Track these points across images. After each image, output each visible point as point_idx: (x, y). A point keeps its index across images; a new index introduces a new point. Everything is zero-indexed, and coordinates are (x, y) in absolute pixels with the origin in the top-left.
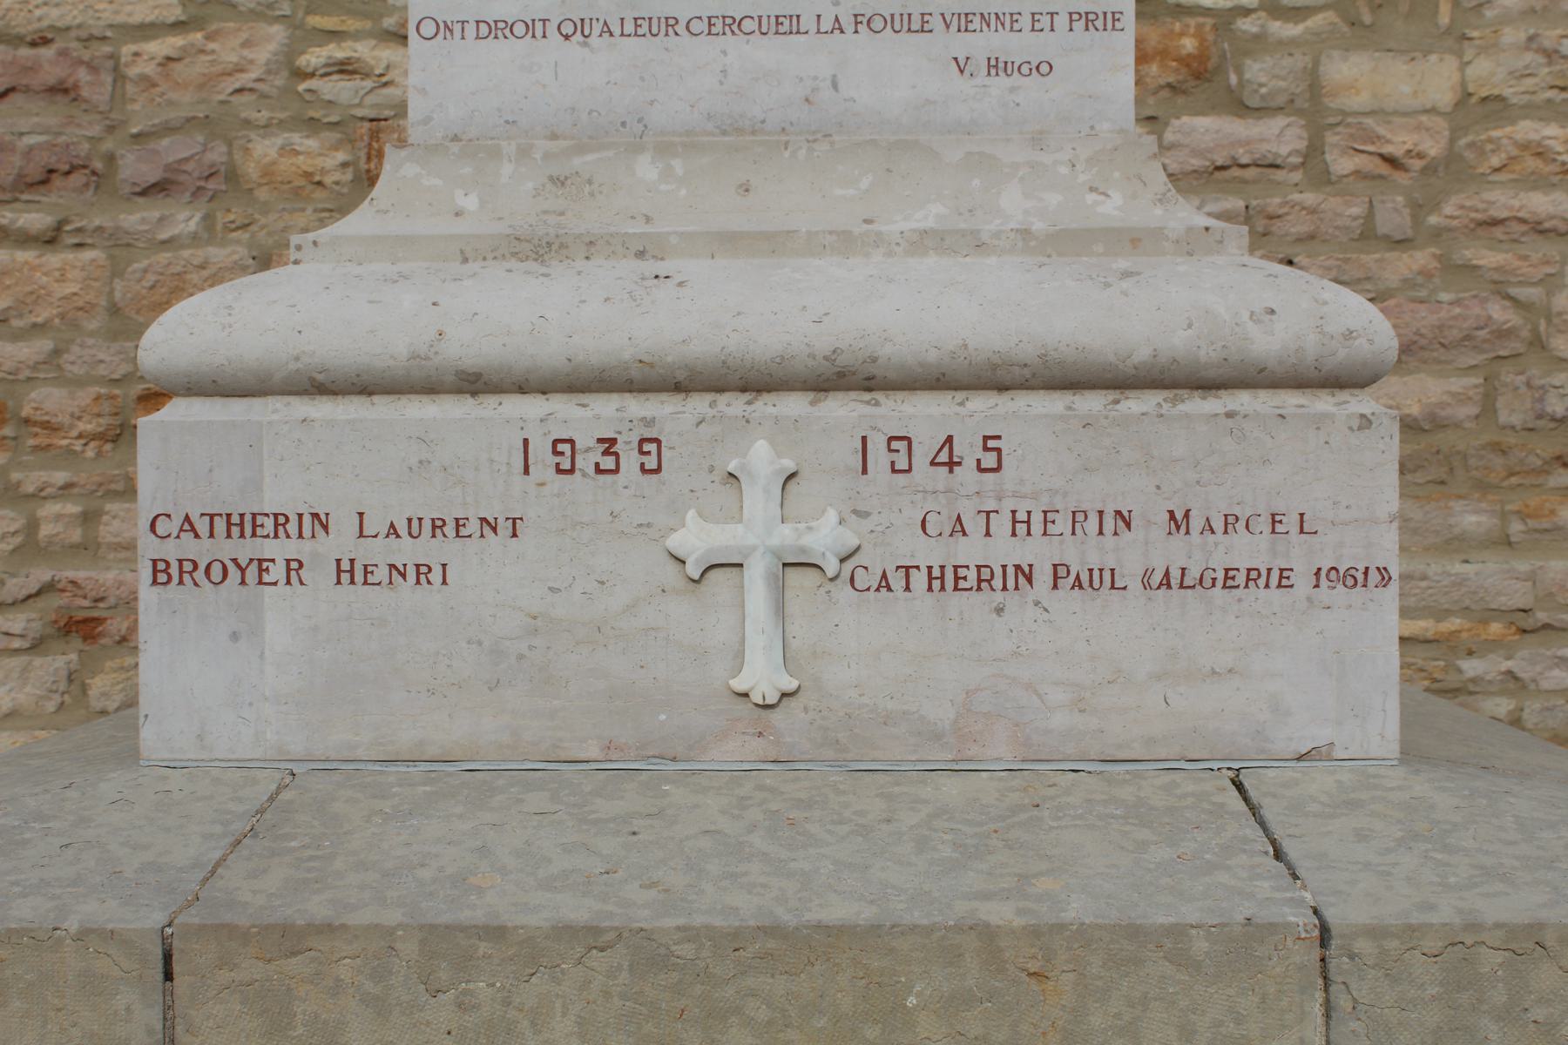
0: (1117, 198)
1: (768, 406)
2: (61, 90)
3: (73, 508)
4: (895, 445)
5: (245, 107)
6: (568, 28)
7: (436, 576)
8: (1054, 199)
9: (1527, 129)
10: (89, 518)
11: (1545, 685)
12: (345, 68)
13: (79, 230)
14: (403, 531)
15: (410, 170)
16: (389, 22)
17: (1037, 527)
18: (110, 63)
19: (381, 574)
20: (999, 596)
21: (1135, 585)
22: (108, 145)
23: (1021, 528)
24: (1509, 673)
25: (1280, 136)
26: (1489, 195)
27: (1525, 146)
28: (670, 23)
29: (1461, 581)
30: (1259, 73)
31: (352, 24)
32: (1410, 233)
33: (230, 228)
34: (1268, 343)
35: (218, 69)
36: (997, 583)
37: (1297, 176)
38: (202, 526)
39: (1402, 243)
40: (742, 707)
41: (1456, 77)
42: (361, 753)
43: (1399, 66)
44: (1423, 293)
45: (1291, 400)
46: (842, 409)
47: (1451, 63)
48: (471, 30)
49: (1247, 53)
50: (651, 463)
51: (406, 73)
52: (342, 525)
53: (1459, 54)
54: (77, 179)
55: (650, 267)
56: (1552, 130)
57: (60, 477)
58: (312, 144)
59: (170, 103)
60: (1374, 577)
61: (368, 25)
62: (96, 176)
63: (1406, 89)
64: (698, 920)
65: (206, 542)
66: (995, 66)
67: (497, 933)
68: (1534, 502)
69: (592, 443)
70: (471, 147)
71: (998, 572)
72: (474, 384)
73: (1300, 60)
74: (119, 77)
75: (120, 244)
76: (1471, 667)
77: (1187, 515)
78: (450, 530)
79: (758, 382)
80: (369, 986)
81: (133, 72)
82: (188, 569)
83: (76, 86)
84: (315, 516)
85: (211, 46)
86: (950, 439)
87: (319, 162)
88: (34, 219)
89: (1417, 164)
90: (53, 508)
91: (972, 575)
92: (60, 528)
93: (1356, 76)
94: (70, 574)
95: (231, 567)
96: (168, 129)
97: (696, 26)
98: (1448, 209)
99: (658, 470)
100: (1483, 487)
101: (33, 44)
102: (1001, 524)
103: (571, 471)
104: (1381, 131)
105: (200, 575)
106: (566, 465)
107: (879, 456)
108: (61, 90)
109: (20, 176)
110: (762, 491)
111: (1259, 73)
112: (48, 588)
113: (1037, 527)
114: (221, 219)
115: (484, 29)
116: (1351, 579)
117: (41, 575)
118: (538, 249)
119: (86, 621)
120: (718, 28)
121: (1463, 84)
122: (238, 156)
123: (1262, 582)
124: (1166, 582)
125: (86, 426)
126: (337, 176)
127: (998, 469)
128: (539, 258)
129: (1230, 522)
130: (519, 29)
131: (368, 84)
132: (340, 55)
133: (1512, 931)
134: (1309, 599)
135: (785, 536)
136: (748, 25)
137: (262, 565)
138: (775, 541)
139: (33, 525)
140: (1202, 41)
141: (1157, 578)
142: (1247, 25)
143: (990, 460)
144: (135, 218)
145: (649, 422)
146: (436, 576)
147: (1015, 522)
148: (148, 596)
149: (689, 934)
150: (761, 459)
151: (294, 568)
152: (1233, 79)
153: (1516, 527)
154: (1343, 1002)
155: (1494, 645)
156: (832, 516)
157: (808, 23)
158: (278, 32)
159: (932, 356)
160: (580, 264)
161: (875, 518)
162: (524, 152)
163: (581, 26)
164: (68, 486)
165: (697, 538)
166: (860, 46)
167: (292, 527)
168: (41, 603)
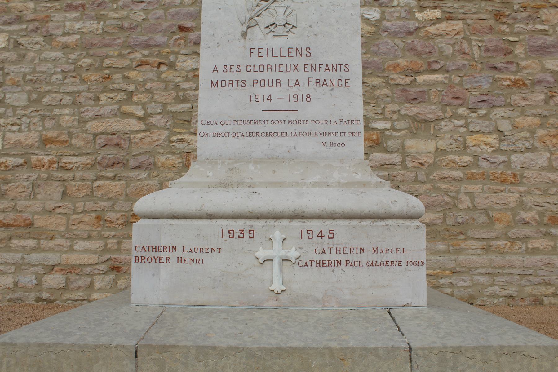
0: (360, 175)
1: (280, 223)
2: (117, 145)
3: (115, 241)
4: (309, 232)
5: (159, 149)
6: (234, 135)
7: (201, 262)
8: (345, 175)
9: (451, 157)
10: (119, 243)
11: (459, 285)
12: (181, 141)
13: (120, 177)
14: (193, 250)
15: (197, 166)
16: (192, 130)
17: (342, 252)
18: (129, 139)
19: (188, 261)
20: (333, 268)
21: (365, 265)
22: (127, 157)
23: (338, 252)
24: (450, 282)
25: (396, 158)
26: (444, 172)
27: (451, 161)
28: (257, 134)
29: (439, 261)
30: (391, 143)
31: (183, 131)
32: (426, 180)
34: (395, 209)
35: (152, 140)
36: (333, 265)
37: (400, 167)
38: (147, 250)
40: (272, 293)
41: (435, 145)
42: (182, 303)
43: (422, 142)
44: (429, 194)
45: (401, 222)
46: (296, 224)
47: (434, 142)
48: (212, 135)
49: (388, 139)
50: (252, 236)
51: (196, 141)
53: (436, 140)
54: (120, 165)
55: (252, 190)
56: (457, 157)
57: (113, 233)
58: (173, 157)
59: (142, 148)
60: (420, 263)
61: (187, 131)
62: (124, 164)
63: (424, 147)
64: (262, 346)
65: (147, 253)
66: (332, 144)
67: (214, 348)
68: (455, 242)
69: (238, 231)
70: (211, 161)
71: (333, 262)
72: (210, 217)
73: (400, 141)
74: (130, 142)
75: (129, 180)
76: (442, 281)
77: (377, 249)
78: (204, 251)
79: (277, 217)
80: (184, 360)
81: (134, 141)
82: (143, 259)
83: (121, 144)
84: (173, 247)
85: (151, 135)
86: (322, 231)
87: (175, 162)
89: (427, 165)
90: (111, 241)
91: (327, 263)
92: (112, 245)
93: (413, 144)
94: (114, 256)
95: (153, 259)
96: (141, 154)
97: (263, 134)
98: (434, 175)
99: (253, 237)
100: (444, 239)
101: (112, 135)
102: (333, 251)
103: (233, 237)
104: (419, 157)
105: (146, 260)
106: (232, 236)
107: (305, 235)
108: (117, 145)
109: (107, 164)
110: (278, 243)
111: (391, 143)
112: (109, 259)
113: (342, 252)
114: (152, 174)
115: (215, 135)
116: (415, 264)
118: (225, 185)
119: (117, 267)
120: (268, 135)
121: (437, 147)
122: (156, 160)
123: (394, 265)
124: (372, 265)
125: (118, 222)
126: (178, 165)
127: (333, 238)
128: (226, 187)
129: (387, 250)
130: (223, 135)
131: (186, 144)
132: (180, 138)
133: (454, 348)
134: (406, 269)
135: (283, 253)
136: (275, 134)
137: (160, 258)
138: (280, 255)
139: (106, 245)
140: (378, 136)
141: (370, 263)
142: (388, 133)
143: (331, 236)
144: (133, 174)
145: (251, 226)
146: (201, 262)
147: (337, 250)
148: (133, 264)
149: (260, 349)
150: (277, 235)
151: (168, 259)
152: (385, 145)
153: (451, 248)
154: (415, 365)
155: (447, 276)
156: (294, 248)
157: (289, 134)
158: (166, 132)
159: (318, 211)
160: (236, 189)
161: (304, 249)
162: (223, 163)
163: (237, 134)
164: (115, 236)
165: (262, 254)
166: (300, 139)
167: (167, 250)
168: (107, 263)
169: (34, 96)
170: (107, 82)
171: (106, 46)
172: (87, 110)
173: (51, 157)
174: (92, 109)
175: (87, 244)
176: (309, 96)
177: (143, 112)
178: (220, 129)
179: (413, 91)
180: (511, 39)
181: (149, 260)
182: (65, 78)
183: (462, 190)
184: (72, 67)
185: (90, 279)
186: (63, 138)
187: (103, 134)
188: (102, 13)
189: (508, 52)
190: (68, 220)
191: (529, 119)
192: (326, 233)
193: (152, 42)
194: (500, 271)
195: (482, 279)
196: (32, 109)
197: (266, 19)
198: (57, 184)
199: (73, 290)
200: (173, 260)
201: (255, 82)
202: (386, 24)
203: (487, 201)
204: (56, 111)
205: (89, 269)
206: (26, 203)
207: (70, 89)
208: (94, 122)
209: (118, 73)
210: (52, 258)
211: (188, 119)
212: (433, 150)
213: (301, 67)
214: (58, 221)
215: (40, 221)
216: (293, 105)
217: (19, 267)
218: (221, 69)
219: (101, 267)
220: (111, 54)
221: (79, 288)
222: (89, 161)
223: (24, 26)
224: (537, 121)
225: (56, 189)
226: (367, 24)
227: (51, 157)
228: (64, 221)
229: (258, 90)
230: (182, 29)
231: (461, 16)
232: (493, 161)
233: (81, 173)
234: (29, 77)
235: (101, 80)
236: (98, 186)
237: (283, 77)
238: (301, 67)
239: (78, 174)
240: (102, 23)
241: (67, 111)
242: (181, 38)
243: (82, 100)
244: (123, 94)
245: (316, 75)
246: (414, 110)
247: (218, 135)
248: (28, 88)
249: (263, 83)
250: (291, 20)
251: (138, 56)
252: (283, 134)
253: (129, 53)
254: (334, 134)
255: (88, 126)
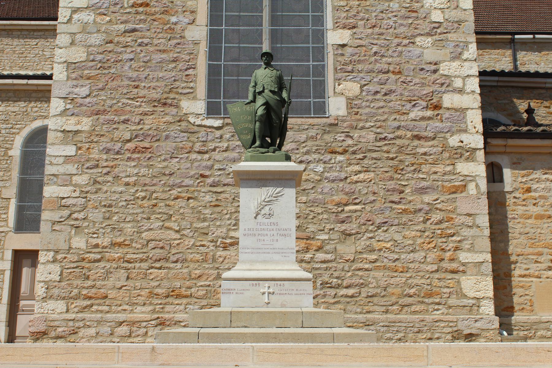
2: (162, 248)
12: (203, 246)
33: (185, 267)
39: (348, 272)
52: (236, 289)
54: (164, 260)
57: (159, 302)
62: (167, 260)
88: (158, 265)
90: (159, 306)
93: (341, 248)
112: (158, 318)
114: (184, 266)
117: (156, 316)
139: (155, 309)
144: (172, 265)
150: (267, 285)
165: (262, 291)
169: (107, 215)
170: (155, 208)
171: (153, 185)
172: (143, 225)
173: (119, 254)
174: (146, 224)
175: (144, 309)
176: (277, 240)
177: (178, 228)
178: (247, 251)
179: (343, 216)
180: (403, 183)
181: (227, 293)
182: (128, 204)
183: (371, 276)
184: (132, 198)
185: (145, 330)
186: (126, 243)
187: (153, 240)
188: (151, 163)
189: (402, 192)
190: (130, 294)
191: (414, 233)
192: (282, 285)
193: (183, 184)
194: (393, 324)
195: (382, 329)
196: (107, 224)
197: (263, 212)
198: (123, 271)
199: (135, 337)
200: (235, 293)
201: (259, 235)
202: (326, 174)
203: (386, 283)
204: (122, 225)
205: (144, 324)
206: (103, 283)
207: (131, 211)
208: (147, 233)
209: (162, 202)
210: (121, 317)
211: (207, 232)
212: (354, 252)
213: (275, 229)
214: (124, 294)
215: (112, 294)
216: (272, 243)
217: (99, 322)
218: (247, 230)
219: (153, 322)
220: (158, 190)
221: (139, 335)
222: (144, 257)
223: (100, 171)
224: (419, 234)
225: (123, 274)
226: (316, 175)
227: (119, 254)
228: (128, 295)
229: (260, 237)
230: (202, 176)
231: (372, 169)
232: (391, 258)
233: (139, 264)
234: (103, 203)
235: (151, 207)
236: (151, 273)
237: (269, 233)
238: (275, 229)
239: (137, 265)
240: (151, 170)
241: (129, 225)
242: (201, 182)
243: (139, 219)
244: (166, 215)
245: (280, 232)
246: (344, 227)
247: (246, 253)
248: (103, 210)
249: (262, 235)
250: (271, 212)
251: (174, 192)
252: (269, 253)
253: (169, 190)
254: (286, 253)
255: (144, 235)
